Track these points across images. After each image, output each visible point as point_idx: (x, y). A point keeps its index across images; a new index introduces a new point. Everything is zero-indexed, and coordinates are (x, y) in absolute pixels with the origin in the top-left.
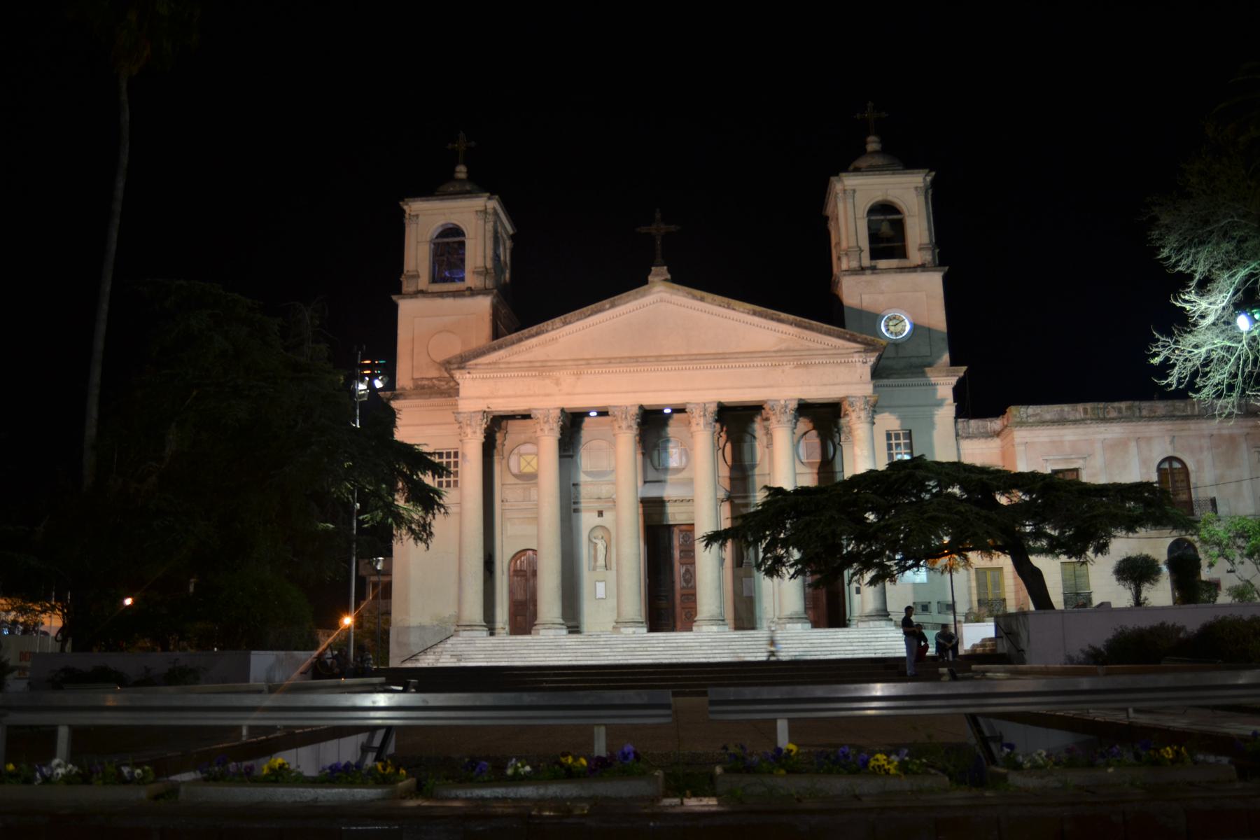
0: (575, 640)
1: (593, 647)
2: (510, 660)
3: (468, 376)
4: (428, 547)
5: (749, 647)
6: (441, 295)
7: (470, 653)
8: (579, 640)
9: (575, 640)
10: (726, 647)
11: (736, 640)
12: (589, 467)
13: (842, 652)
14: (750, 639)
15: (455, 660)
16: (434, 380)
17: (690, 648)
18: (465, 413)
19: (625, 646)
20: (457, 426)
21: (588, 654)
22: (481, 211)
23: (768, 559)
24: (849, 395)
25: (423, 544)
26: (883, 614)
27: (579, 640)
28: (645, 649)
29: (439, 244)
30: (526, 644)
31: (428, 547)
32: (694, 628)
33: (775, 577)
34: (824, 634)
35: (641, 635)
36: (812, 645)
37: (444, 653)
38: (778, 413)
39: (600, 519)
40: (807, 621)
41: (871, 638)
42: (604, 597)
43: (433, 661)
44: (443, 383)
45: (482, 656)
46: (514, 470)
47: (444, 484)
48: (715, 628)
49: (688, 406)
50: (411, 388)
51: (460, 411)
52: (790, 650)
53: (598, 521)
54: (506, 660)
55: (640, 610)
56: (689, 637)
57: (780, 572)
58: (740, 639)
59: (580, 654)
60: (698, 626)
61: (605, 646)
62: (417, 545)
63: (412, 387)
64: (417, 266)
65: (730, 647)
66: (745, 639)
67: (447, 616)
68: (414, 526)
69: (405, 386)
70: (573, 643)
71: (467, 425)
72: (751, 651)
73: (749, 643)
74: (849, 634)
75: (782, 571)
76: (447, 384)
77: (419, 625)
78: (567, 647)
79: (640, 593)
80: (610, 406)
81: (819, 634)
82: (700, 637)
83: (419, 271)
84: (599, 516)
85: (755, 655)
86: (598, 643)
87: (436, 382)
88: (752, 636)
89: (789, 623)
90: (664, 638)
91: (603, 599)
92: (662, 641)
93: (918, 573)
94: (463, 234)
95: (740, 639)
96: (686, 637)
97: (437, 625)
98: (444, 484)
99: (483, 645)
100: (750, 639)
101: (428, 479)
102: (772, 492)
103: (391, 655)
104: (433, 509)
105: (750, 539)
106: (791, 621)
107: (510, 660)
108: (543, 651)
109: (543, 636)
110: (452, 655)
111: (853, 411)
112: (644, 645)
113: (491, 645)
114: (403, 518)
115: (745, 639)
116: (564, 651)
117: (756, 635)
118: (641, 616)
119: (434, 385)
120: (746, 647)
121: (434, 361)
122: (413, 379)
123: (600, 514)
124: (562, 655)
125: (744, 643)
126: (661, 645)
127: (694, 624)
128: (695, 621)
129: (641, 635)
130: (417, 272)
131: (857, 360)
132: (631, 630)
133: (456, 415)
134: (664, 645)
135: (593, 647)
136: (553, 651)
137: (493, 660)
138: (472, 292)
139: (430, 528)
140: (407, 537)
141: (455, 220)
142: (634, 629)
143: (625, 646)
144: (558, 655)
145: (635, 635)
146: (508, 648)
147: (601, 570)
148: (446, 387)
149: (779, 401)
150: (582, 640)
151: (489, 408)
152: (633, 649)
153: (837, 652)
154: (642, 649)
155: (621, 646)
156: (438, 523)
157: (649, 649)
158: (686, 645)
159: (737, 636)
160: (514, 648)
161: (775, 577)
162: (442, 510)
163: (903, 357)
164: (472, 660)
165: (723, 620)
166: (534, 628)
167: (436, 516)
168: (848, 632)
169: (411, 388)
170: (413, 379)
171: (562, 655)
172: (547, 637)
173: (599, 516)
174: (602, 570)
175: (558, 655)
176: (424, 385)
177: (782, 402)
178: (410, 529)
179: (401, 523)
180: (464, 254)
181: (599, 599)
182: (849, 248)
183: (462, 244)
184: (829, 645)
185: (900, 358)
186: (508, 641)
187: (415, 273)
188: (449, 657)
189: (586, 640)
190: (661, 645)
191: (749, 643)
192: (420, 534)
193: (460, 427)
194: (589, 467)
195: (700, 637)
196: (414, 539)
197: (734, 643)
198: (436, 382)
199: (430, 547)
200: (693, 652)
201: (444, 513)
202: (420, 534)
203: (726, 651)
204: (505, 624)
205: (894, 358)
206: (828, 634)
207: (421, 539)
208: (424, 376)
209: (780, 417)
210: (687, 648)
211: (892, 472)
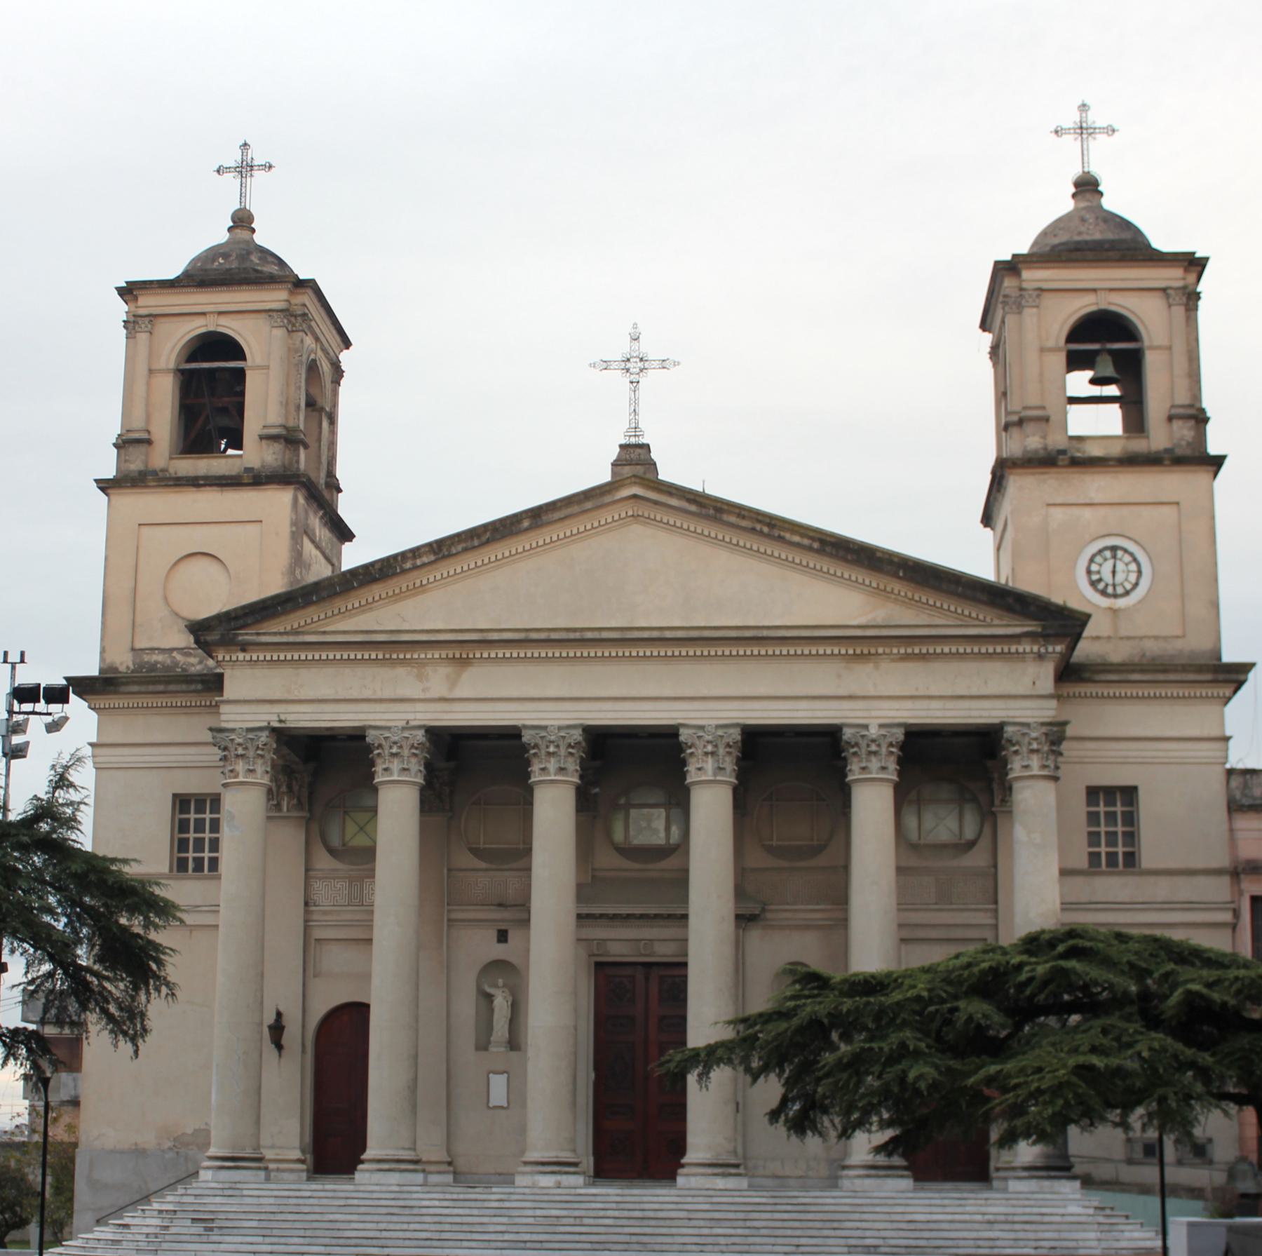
0: (441, 1196)
1: (475, 1212)
2: (309, 1233)
3: (241, 656)
4: (136, 1052)
6: (195, 482)
7: (231, 1216)
8: (448, 1196)
9: (441, 1196)
10: (740, 1224)
11: (762, 1208)
12: (482, 840)
13: (971, 1243)
14: (789, 1208)
15: (201, 1231)
16: (175, 654)
17: (668, 1223)
18: (233, 730)
19: (539, 1212)
20: (221, 753)
21: (465, 1228)
22: (281, 311)
23: (794, 1100)
24: (1006, 720)
25: (129, 1044)
26: (1060, 1163)
27: (448, 1196)
28: (578, 1221)
29: (192, 371)
30: (342, 1202)
31: (136, 1052)
32: (680, 1180)
33: (809, 1133)
34: (938, 1202)
35: (572, 1191)
36: (912, 1226)
37: (179, 1215)
38: (864, 751)
39: (502, 946)
40: (906, 1173)
41: (1024, 1214)
42: (506, 1105)
43: (157, 1230)
44: (193, 660)
45: (254, 1224)
46: (335, 841)
47: (191, 865)
48: (720, 1183)
49: (682, 731)
50: (128, 668)
51: (224, 725)
52: (868, 1233)
53: (499, 951)
54: (302, 1233)
55: (573, 1140)
56: (667, 1199)
57: (819, 1126)
58: (769, 1208)
59: (447, 1227)
60: (687, 1175)
61: (498, 1212)
62: (116, 1046)
63: (132, 667)
64: (148, 418)
65: (749, 1224)
67: (190, 1131)
68: (112, 1009)
69: (117, 664)
70: (437, 1203)
71: (237, 756)
72: (789, 1232)
73: (786, 1216)
74: (986, 1205)
75: (822, 1124)
76: (200, 662)
77: (134, 1147)
78: (424, 1211)
79: (574, 1104)
80: (525, 727)
81: (927, 1202)
82: (689, 1199)
83: (152, 429)
84: (499, 941)
85: (796, 1241)
86: (487, 1204)
87: (178, 657)
88: (795, 1201)
89: (868, 1176)
90: (619, 1199)
91: (502, 1107)
92: (614, 1206)
93: (1092, 1128)
94: (237, 352)
95: (769, 1208)
96: (661, 1199)
97: (170, 1149)
98: (191, 865)
99: (255, 1201)
100: (789, 1208)
101: (135, 924)
102: (796, 978)
103: (76, 1207)
104: (147, 985)
105: (755, 1064)
106: (873, 1172)
107: (309, 1233)
108: (376, 1218)
109: (377, 1185)
110: (193, 1219)
111: (1016, 752)
112: (577, 1213)
113: (272, 1201)
114: (92, 991)
116: (417, 1219)
118: (574, 1151)
119: (176, 664)
121: (177, 614)
122: (133, 649)
123: (503, 936)
124: (412, 1226)
126: (610, 1213)
127: (680, 1171)
128: (683, 1166)
129: (572, 1191)
130: (149, 432)
131: (1028, 649)
132: (547, 1181)
133: (215, 734)
134: (616, 1214)
135: (475, 1212)
136: (395, 1219)
137: (275, 1232)
138: (257, 479)
139: (142, 1021)
140: (99, 1027)
141: (229, 327)
142: (558, 1177)
143: (539, 1212)
144: (405, 1226)
145: (559, 1191)
146: (306, 1209)
147: (498, 1049)
148: (199, 668)
149: (866, 727)
150: (455, 1196)
151: (281, 721)
152: (554, 1221)
154: (572, 1221)
155: (530, 1213)
156: (156, 1008)
157: (586, 1221)
158: (660, 1214)
159: (764, 1200)
160: (317, 1209)
161: (809, 1133)
162: (164, 990)
163: (1128, 638)
164: (235, 1231)
165: (737, 1166)
166: (360, 1167)
167: (152, 1001)
168: (986, 1199)
169: (128, 668)
170: (133, 649)
171: (412, 1226)
172: (384, 1188)
173: (499, 941)
174: (503, 1049)
175: (405, 1226)
176: (157, 662)
177: (874, 731)
178: (105, 1012)
179: (88, 1000)
180: (242, 394)
181: (495, 1107)
182: (1025, 408)
183: (240, 375)
185: (1121, 638)
186: (308, 1194)
187: (144, 436)
188: (189, 1223)
189: (461, 1196)
190: (610, 1213)
191: (786, 1216)
192: (125, 1024)
193: (224, 759)
194: (482, 840)
195: (689, 1199)
196: (111, 1031)
198: (178, 657)
199: (140, 1052)
200: (674, 1231)
201: (168, 994)
202: (125, 1024)
203: (739, 1231)
204: (303, 1151)
205: (1109, 638)
206: (946, 1202)
207: (125, 1034)
208: (155, 645)
209: (868, 761)
210: (662, 1223)
211: (1024, 958)
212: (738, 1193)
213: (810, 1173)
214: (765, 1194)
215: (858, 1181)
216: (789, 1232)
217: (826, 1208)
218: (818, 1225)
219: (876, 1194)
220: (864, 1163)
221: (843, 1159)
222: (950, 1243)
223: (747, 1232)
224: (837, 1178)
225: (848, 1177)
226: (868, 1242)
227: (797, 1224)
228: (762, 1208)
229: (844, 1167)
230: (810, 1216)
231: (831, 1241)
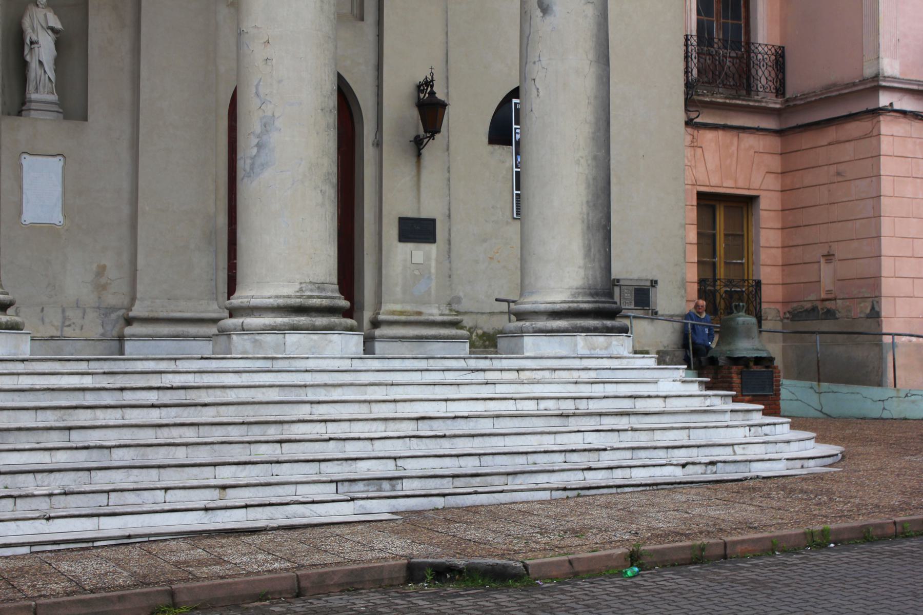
5: (165, 435)
10: (55, 439)
11: (90, 399)
14: (152, 397)
58: (107, 399)
65: (77, 438)
66: (130, 397)
72: (180, 455)
73: (154, 416)
88: (154, 381)
89: (295, 328)
95: (107, 399)
100: (152, 397)
106: (302, 320)
115: (130, 397)
117: (168, 380)
120: (147, 436)
125: (134, 416)
153: (543, 461)
159: (87, 381)
184: (485, 426)
191: (154, 416)
197: (83, 418)
203: (62, 459)
212: (19, 367)
213: (68, 332)
214: (83, 367)
215: (269, 339)
216: (180, 455)
217: (231, 396)
218: (235, 433)
219: (311, 364)
220: (281, 302)
221: (129, 309)
222: (520, 463)
223: (81, 459)
224: (121, 339)
225: (243, 330)
226: (363, 469)
227: (189, 435)
228: (90, 399)
229: (129, 321)
230: (208, 415)
231: (286, 472)
